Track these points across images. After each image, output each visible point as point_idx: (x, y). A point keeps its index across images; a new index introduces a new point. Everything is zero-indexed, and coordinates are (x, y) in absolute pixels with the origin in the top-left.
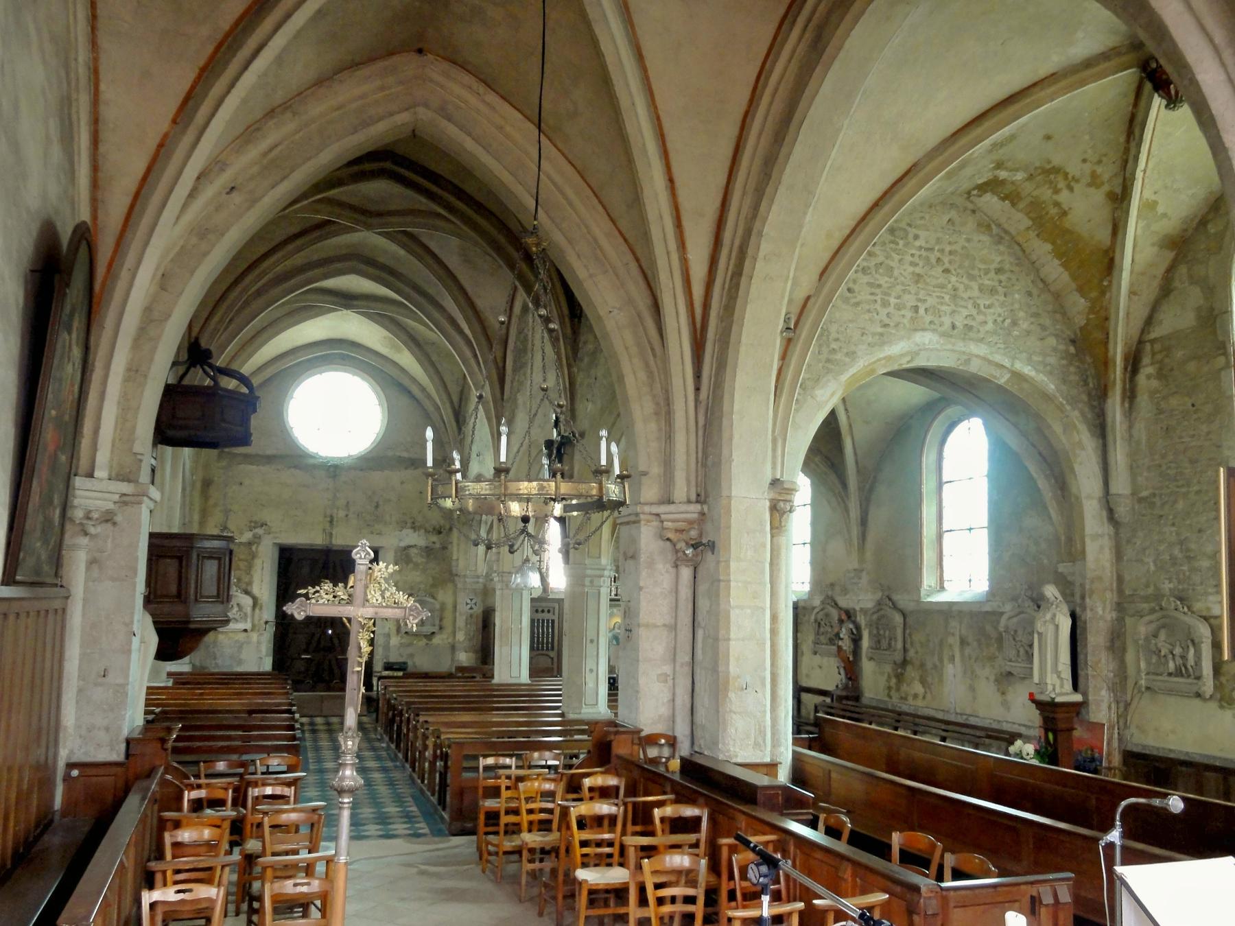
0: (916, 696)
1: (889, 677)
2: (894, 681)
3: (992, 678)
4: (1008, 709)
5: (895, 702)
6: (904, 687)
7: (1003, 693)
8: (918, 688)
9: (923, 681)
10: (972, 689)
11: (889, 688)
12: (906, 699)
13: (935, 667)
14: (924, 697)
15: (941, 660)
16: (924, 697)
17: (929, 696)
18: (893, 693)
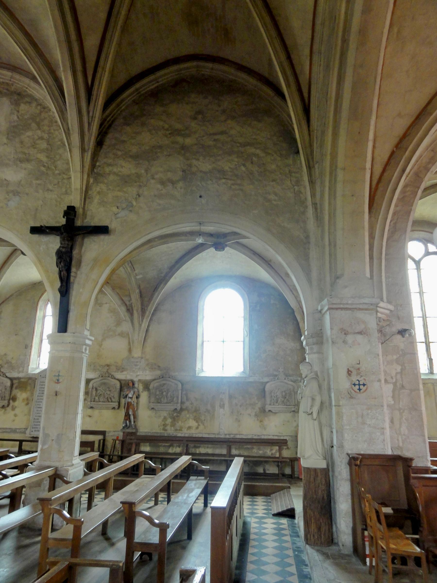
0: (189, 428)
1: (165, 418)
2: (169, 421)
3: (254, 414)
4: (265, 429)
5: (170, 431)
6: (179, 424)
7: (261, 421)
8: (192, 423)
9: (197, 419)
10: (238, 420)
11: (165, 425)
12: (181, 430)
13: (208, 411)
14: (197, 428)
15: (213, 407)
16: (197, 428)
17: (201, 427)
18: (168, 428)
